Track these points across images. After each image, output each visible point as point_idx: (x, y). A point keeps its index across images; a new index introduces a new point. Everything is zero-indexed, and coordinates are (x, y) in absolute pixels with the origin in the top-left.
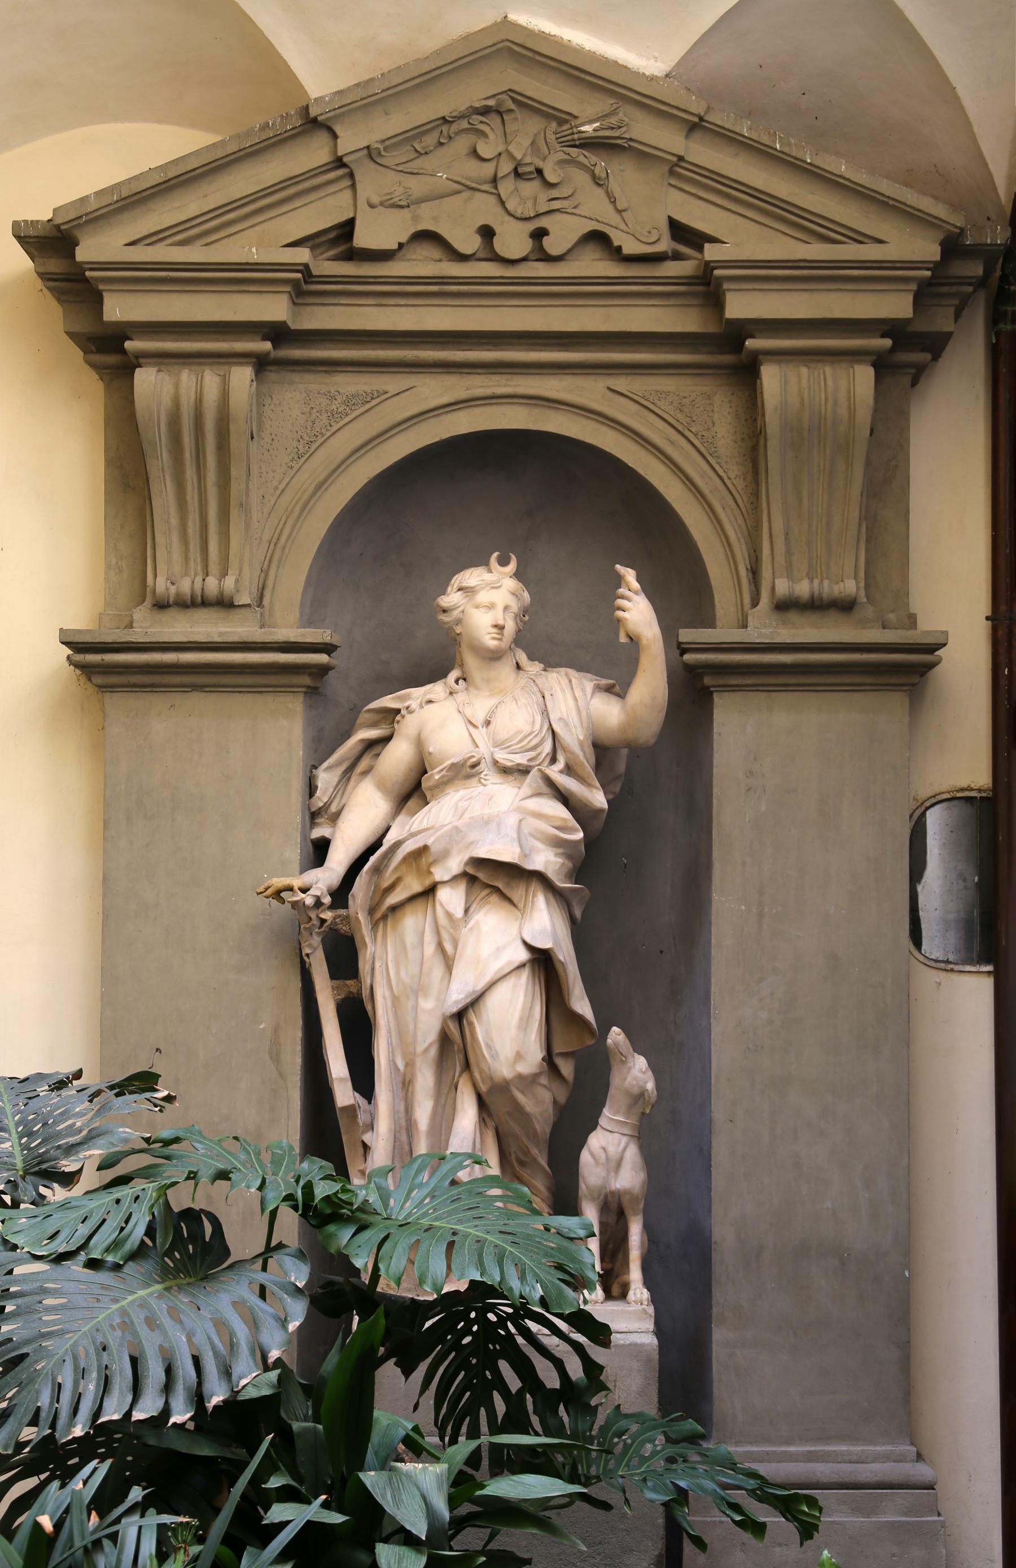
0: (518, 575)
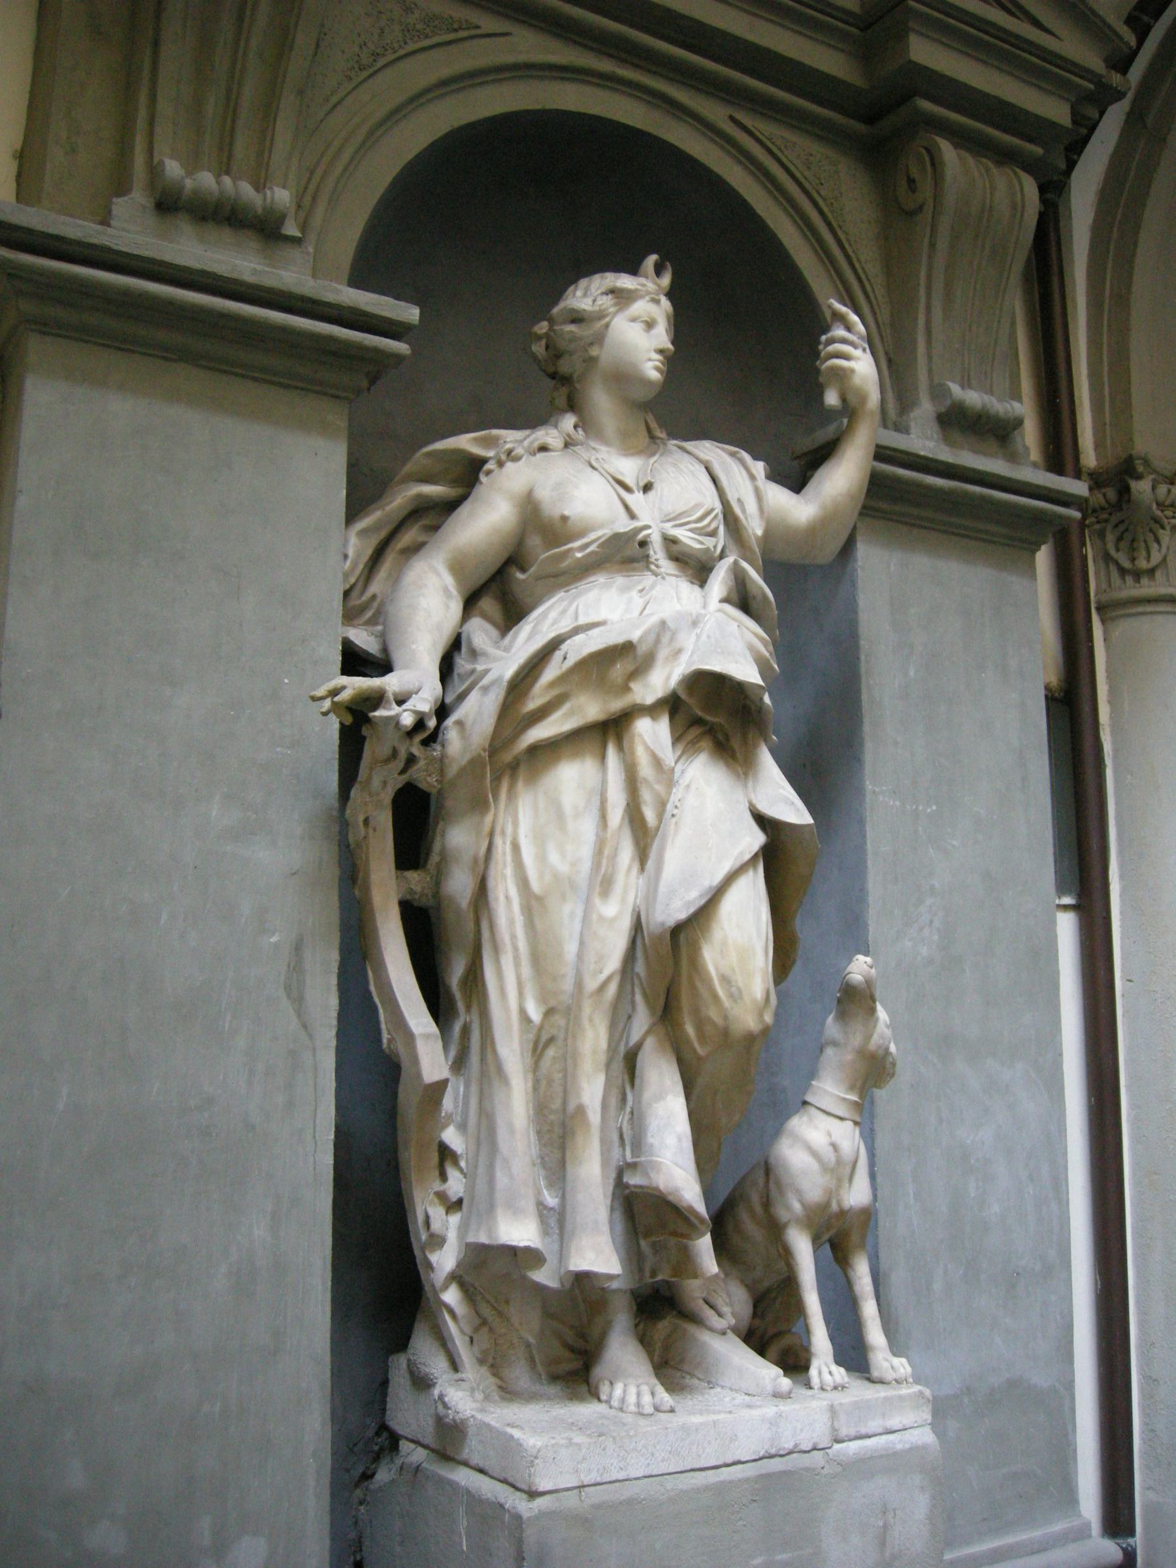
0: (671, 294)
